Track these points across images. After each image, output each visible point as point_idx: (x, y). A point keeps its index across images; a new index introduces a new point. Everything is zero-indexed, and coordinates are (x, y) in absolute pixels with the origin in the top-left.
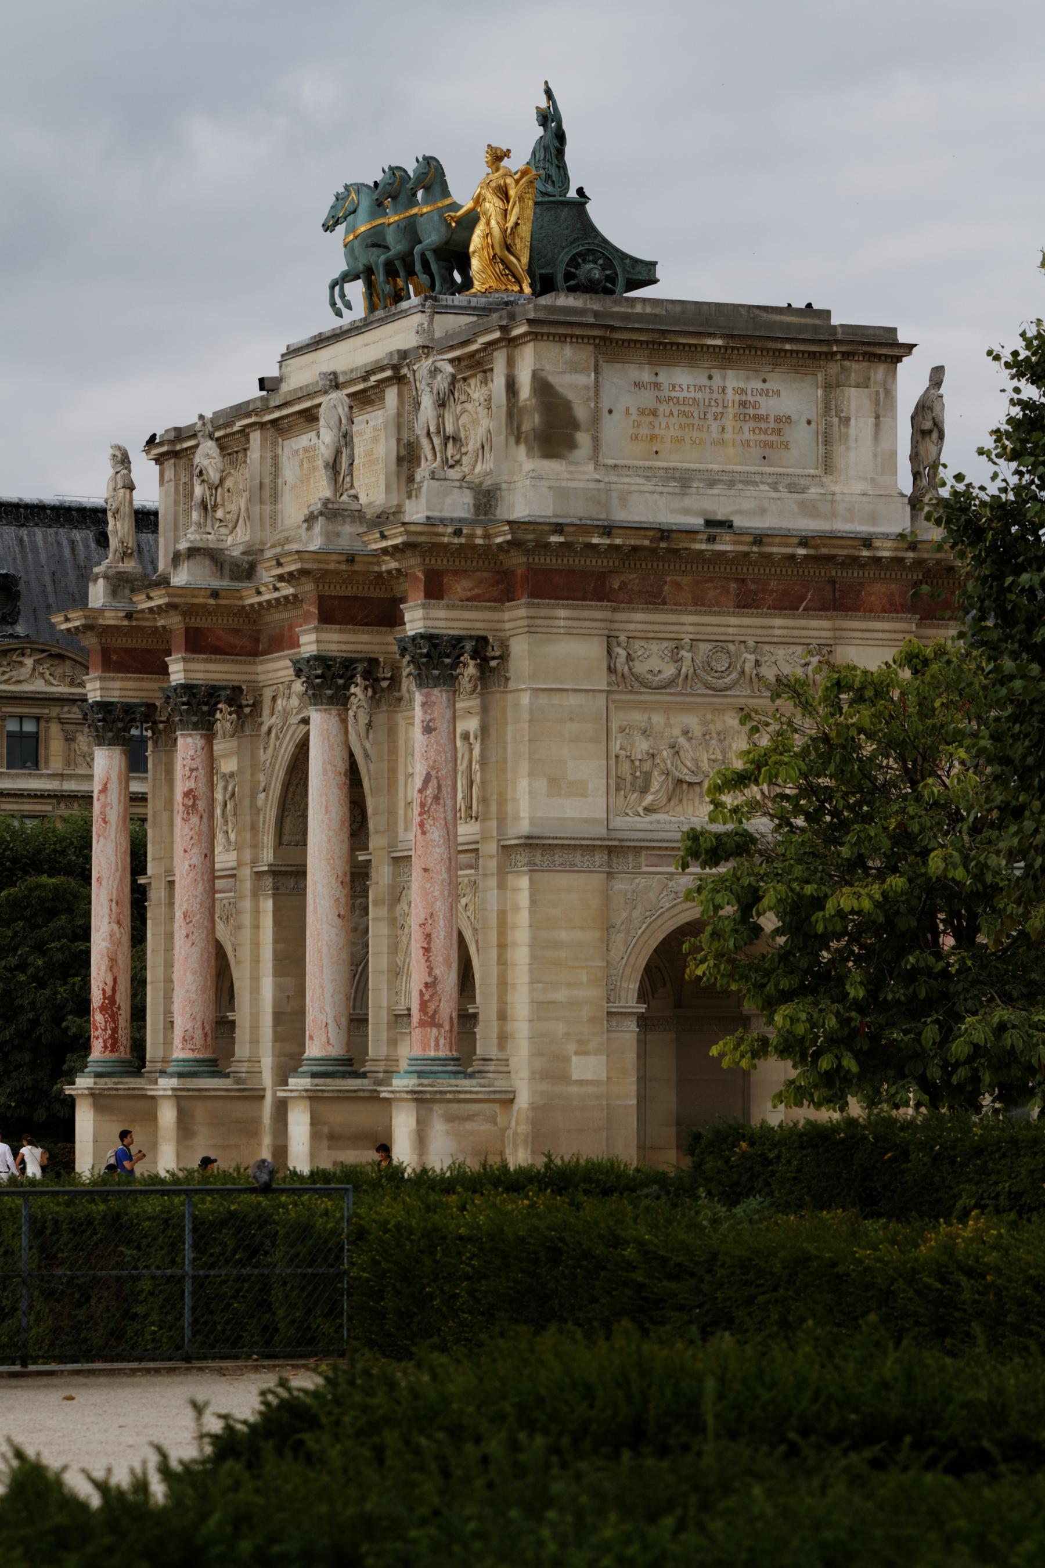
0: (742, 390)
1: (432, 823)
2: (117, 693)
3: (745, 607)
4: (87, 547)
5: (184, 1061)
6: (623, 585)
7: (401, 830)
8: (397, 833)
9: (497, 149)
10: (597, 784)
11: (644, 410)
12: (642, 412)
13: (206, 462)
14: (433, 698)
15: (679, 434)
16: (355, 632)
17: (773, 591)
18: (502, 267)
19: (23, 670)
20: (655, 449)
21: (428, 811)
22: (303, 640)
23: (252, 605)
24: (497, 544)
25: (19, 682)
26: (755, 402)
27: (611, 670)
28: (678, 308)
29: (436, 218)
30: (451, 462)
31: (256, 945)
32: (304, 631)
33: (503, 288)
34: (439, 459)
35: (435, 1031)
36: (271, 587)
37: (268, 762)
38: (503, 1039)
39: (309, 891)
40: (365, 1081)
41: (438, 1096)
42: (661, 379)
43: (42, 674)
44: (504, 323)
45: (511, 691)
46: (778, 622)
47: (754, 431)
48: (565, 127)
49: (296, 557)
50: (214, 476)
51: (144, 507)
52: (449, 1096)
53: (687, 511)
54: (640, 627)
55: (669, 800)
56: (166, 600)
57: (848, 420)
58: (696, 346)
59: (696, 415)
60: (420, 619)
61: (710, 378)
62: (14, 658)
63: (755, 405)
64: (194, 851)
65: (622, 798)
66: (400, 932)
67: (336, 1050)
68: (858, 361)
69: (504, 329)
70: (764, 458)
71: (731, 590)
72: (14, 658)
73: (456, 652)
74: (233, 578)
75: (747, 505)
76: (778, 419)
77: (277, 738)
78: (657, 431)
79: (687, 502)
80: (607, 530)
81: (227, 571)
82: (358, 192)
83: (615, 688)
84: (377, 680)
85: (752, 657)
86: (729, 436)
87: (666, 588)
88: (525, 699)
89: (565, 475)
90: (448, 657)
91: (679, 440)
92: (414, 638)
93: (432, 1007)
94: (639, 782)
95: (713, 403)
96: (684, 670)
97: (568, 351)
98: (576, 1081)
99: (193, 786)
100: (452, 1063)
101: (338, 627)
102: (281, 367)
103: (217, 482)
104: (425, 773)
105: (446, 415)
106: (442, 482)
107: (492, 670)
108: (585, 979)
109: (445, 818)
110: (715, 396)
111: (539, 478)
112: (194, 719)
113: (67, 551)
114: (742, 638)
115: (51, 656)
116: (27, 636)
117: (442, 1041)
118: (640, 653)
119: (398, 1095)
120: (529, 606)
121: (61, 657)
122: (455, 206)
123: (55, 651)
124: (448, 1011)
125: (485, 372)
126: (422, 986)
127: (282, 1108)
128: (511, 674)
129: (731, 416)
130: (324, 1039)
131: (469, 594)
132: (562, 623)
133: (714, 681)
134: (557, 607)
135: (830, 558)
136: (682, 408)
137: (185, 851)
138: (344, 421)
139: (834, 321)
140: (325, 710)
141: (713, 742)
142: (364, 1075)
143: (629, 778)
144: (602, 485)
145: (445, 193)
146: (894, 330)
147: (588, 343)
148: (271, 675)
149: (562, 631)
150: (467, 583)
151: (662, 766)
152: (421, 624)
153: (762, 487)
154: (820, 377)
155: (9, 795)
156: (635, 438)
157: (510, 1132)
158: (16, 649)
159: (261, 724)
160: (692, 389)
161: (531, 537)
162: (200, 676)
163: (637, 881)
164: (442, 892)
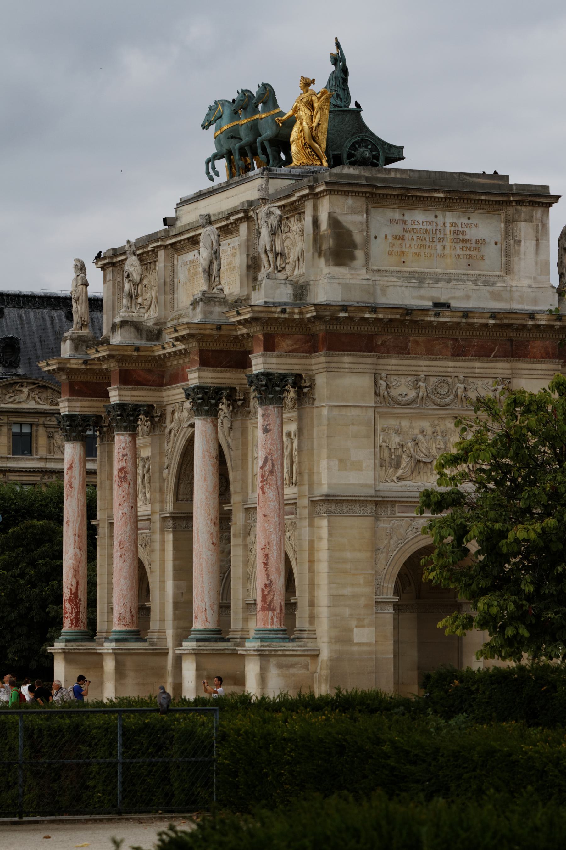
0: (456, 224)
1: (268, 487)
2: (78, 409)
3: (458, 355)
4: (60, 320)
5: (119, 632)
6: (384, 343)
7: (250, 491)
8: (247, 493)
9: (306, 79)
10: (369, 463)
11: (396, 236)
12: (395, 238)
13: (131, 269)
14: (269, 412)
15: (417, 251)
16: (221, 372)
17: (474, 346)
18: (310, 150)
19: (22, 395)
20: (403, 260)
21: (266, 480)
22: (190, 376)
23: (159, 356)
24: (307, 318)
25: (20, 402)
26: (463, 231)
27: (377, 394)
28: (416, 175)
29: (270, 121)
30: (279, 268)
31: (163, 561)
32: (191, 371)
33: (311, 163)
34: (272, 267)
35: (271, 613)
36: (171, 344)
37: (170, 450)
38: (312, 618)
39: (195, 528)
40: (229, 644)
41: (273, 653)
42: (406, 217)
43: (34, 398)
44: (311, 184)
45: (316, 407)
46: (478, 364)
47: (463, 249)
48: (348, 65)
49: (186, 326)
50: (136, 277)
51: (95, 296)
52: (280, 653)
53: (422, 298)
54: (394, 368)
55: (412, 473)
56: (108, 353)
57: (520, 241)
58: (427, 197)
59: (427, 239)
60: (261, 364)
61: (436, 217)
62: (17, 388)
63: (463, 233)
64: (125, 505)
65: (384, 472)
66: (249, 553)
67: (211, 625)
68: (526, 206)
69: (311, 188)
70: (469, 265)
71: (450, 345)
72: (17, 388)
73: (283, 383)
74: (149, 339)
75: (458, 293)
76: (477, 242)
77: (175, 436)
78: (404, 249)
79: (422, 292)
80: (374, 309)
81: (144, 335)
82: (223, 105)
83: (379, 405)
84: (235, 401)
85: (462, 386)
86: (447, 252)
87: (410, 344)
88: (325, 412)
89: (349, 276)
90: (278, 386)
91: (417, 255)
92: (257, 375)
93: (269, 599)
94: (394, 462)
95: (438, 232)
96: (421, 394)
97: (350, 201)
98: (357, 643)
99: (124, 465)
100: (281, 632)
101: (211, 368)
102: (176, 211)
103: (138, 281)
104: (264, 457)
105: (276, 240)
106: (274, 281)
107: (305, 394)
108: (361, 582)
110: (439, 227)
111: (333, 278)
112: (125, 425)
113: (48, 323)
115: (39, 387)
116: (25, 374)
117: (275, 619)
118: (394, 384)
119: (249, 652)
120: (327, 355)
121: (45, 387)
122: (281, 114)
123: (41, 383)
124: (279, 601)
125: (300, 214)
126: (263, 586)
127: (178, 660)
128: (316, 397)
129: (449, 240)
130: (204, 618)
131: (291, 348)
132: (347, 366)
133: (439, 400)
134: (342, 356)
135: (509, 326)
136: (419, 235)
137: (120, 505)
138: (214, 244)
139: (512, 182)
140: (204, 419)
141: (439, 437)
142: (228, 640)
143: (388, 459)
144: (371, 282)
145: (276, 106)
146: (547, 188)
147: (362, 196)
148: (171, 398)
149: (347, 370)
150: (289, 342)
151: (408, 452)
152: (261, 366)
153: (468, 283)
154: (503, 216)
155: (14, 471)
156: (391, 253)
157: (317, 675)
158: (18, 383)
159: (165, 427)
160: (425, 223)
161: (328, 313)
162: (128, 398)
163: (393, 522)
164: (275, 529)
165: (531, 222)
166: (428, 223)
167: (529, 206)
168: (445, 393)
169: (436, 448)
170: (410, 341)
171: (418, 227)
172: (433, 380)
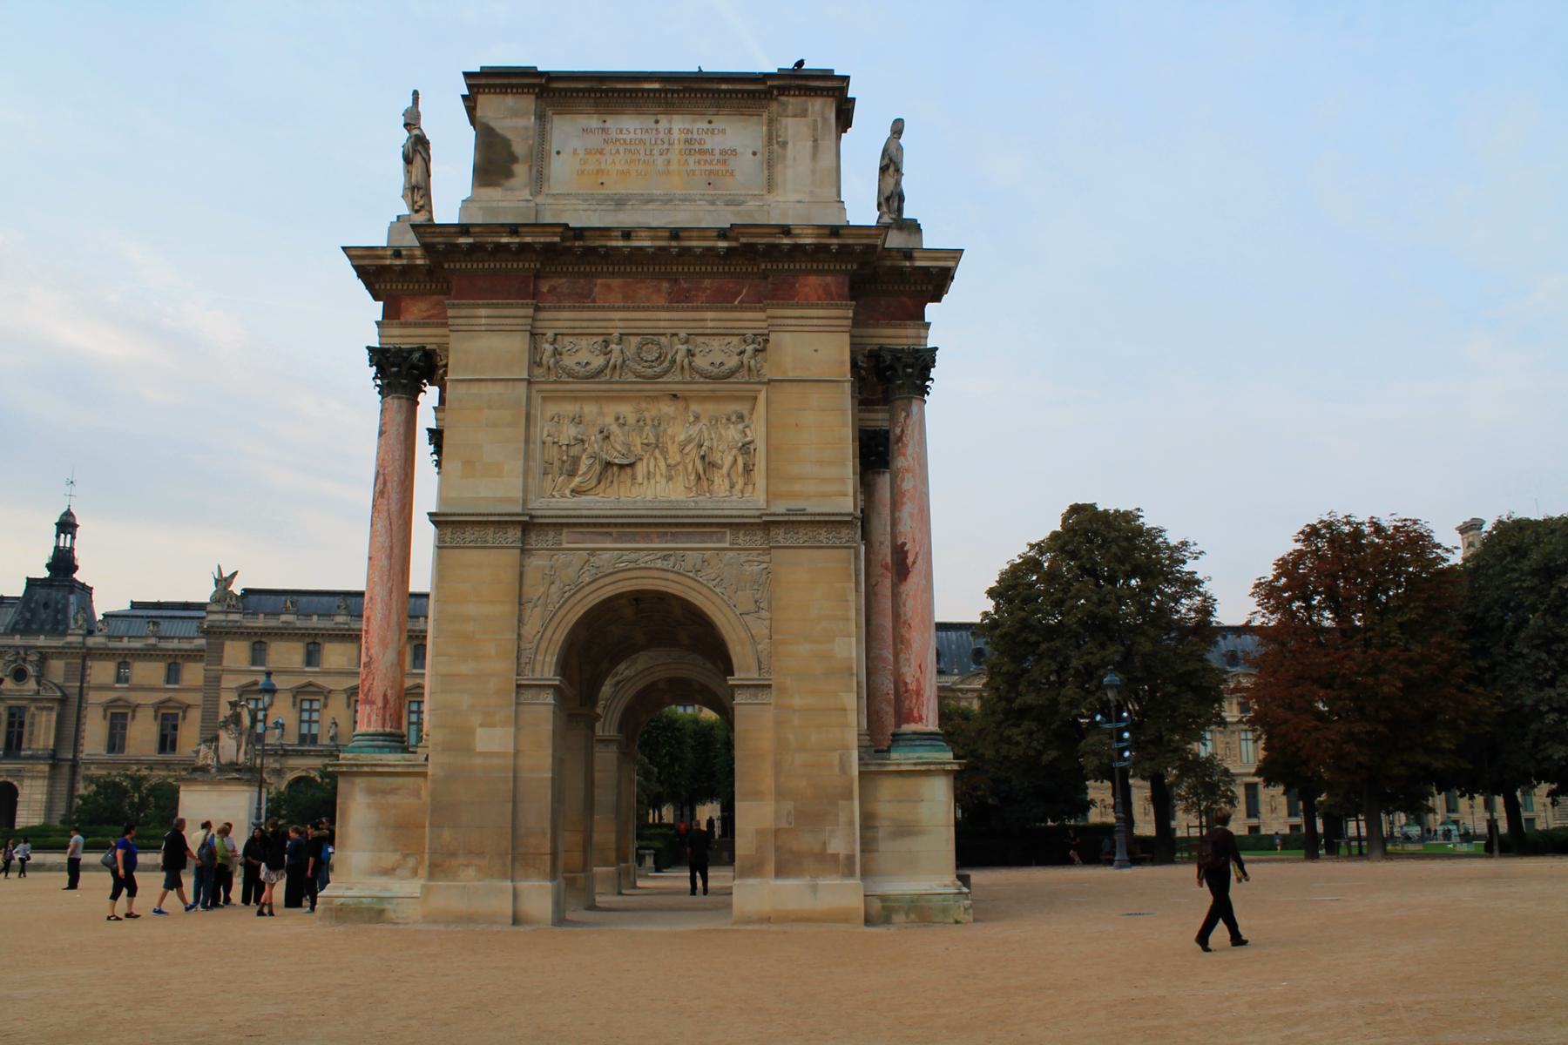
0: (688, 130)
6: (553, 290)
17: (706, 288)
20: (600, 181)
26: (701, 139)
35: (368, 707)
41: (355, 769)
47: (699, 163)
52: (366, 769)
55: (599, 482)
57: (784, 144)
70: (709, 184)
76: (723, 152)
78: (603, 166)
85: (683, 348)
86: (674, 167)
87: (596, 290)
94: (567, 466)
95: (659, 142)
97: (510, 100)
100: (381, 738)
109: (388, 510)
110: (661, 135)
114: (673, 331)
117: (374, 717)
124: (382, 689)
129: (677, 152)
131: (425, 314)
132: (483, 321)
136: (628, 147)
141: (647, 428)
146: (833, 70)
147: (528, 93)
149: (483, 328)
154: (765, 116)
160: (639, 131)
163: (556, 557)
165: (805, 116)
166: (644, 131)
168: (654, 358)
169: (642, 444)
171: (627, 137)
172: (635, 341)
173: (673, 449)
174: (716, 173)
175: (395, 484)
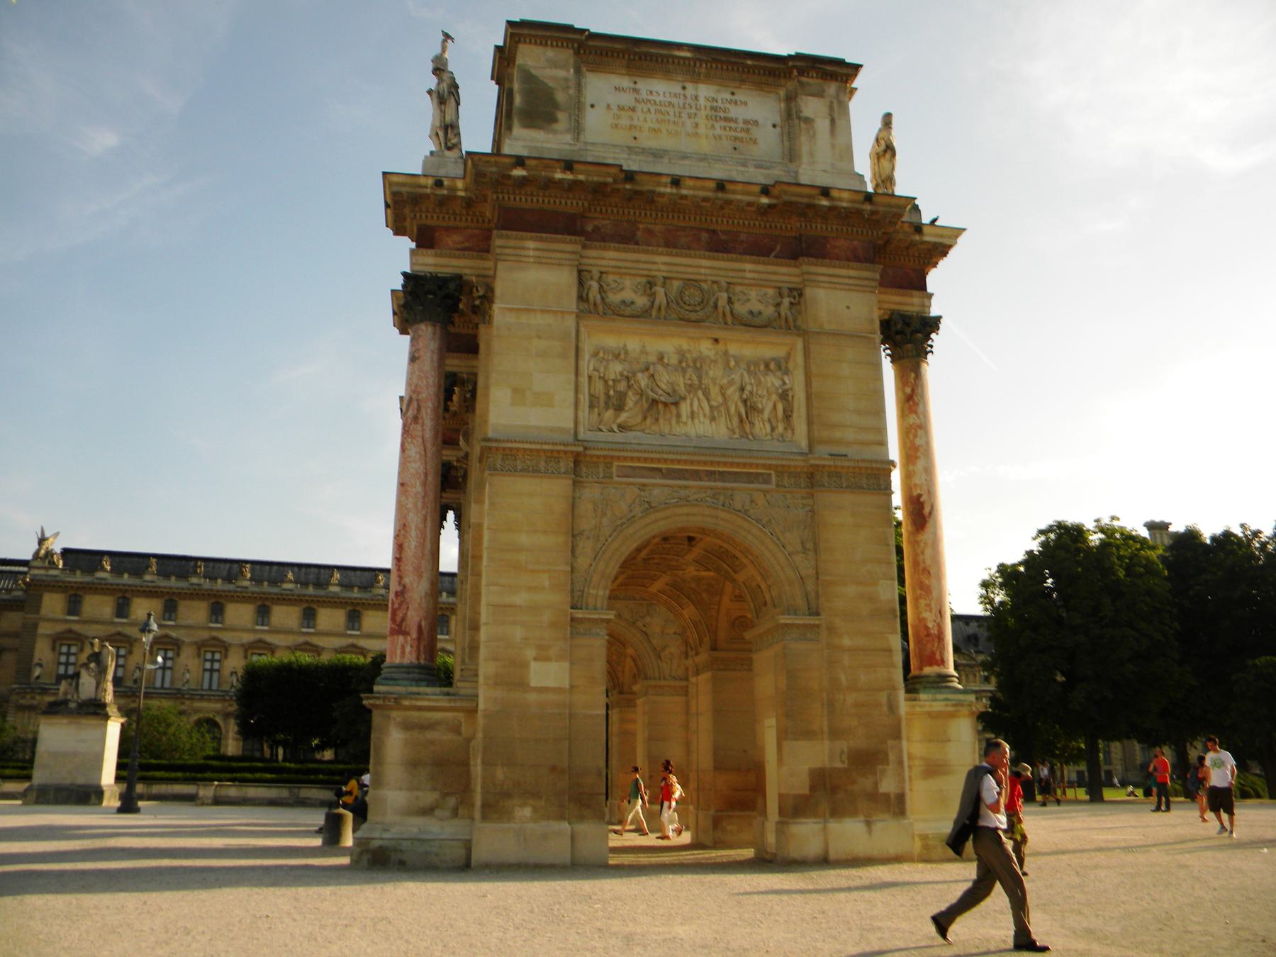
0: (713, 99)
14: (420, 332)
15: (656, 126)
17: (742, 241)
26: (725, 109)
27: (582, 298)
35: (401, 638)
42: (638, 86)
46: (748, 266)
55: (645, 418)
59: (672, 113)
61: (684, 88)
71: (703, 239)
76: (746, 122)
78: (635, 122)
86: (702, 130)
87: (639, 233)
93: (400, 615)
95: (687, 106)
96: (657, 303)
97: (550, 53)
108: (547, 583)
117: (408, 649)
124: (416, 619)
129: (704, 117)
131: (459, 246)
132: (531, 253)
143: (602, 398)
147: (567, 47)
149: (531, 260)
150: (457, 238)
154: (782, 93)
160: (668, 95)
161: (494, 169)
164: (415, 505)
165: (822, 97)
167: (817, 78)
169: (685, 384)
170: (638, 229)
171: (658, 99)
172: (676, 284)
173: (714, 391)
174: (741, 140)
175: (429, 411)
